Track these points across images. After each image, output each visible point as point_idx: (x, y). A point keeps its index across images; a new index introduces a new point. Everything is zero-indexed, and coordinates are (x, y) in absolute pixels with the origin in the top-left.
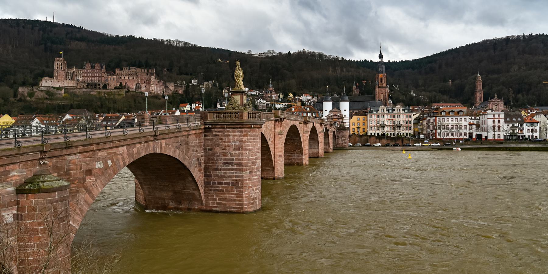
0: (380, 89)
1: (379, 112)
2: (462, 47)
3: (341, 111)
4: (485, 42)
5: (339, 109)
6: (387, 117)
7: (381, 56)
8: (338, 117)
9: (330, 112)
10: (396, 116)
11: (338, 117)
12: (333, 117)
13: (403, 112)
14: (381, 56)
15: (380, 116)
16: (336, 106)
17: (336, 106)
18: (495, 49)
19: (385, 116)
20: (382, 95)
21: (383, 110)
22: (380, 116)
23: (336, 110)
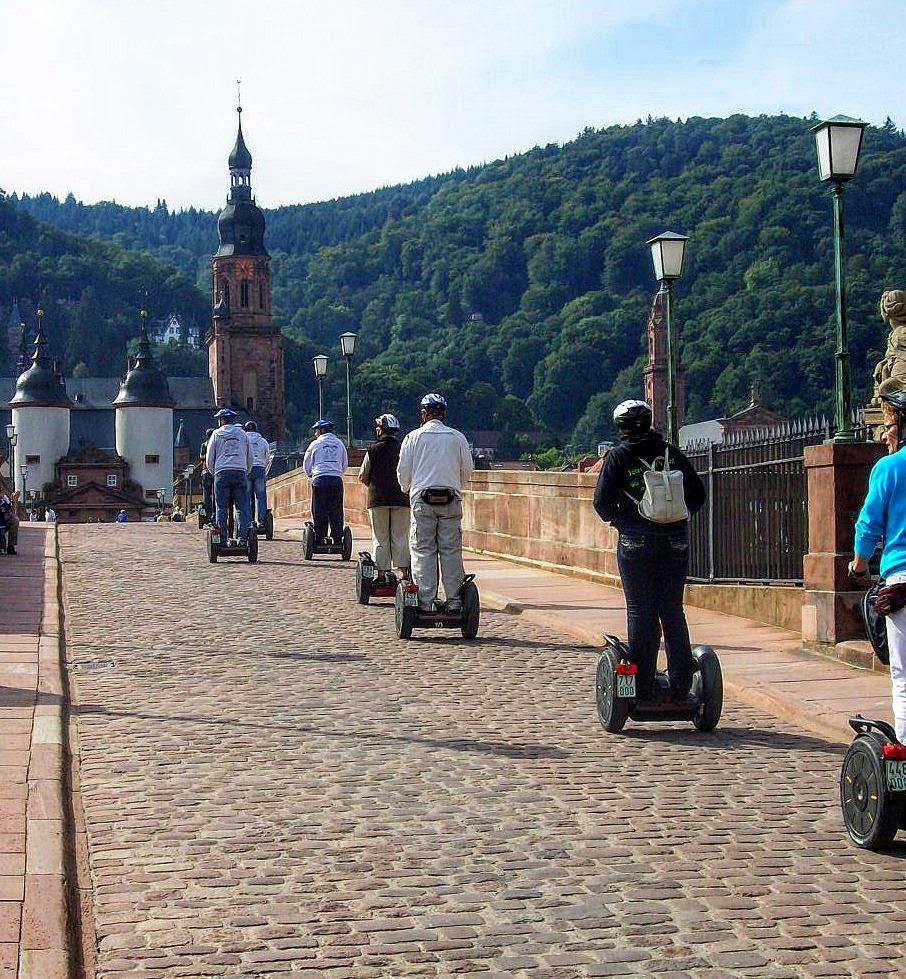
0: (238, 342)
7: (241, 161)
14: (241, 161)
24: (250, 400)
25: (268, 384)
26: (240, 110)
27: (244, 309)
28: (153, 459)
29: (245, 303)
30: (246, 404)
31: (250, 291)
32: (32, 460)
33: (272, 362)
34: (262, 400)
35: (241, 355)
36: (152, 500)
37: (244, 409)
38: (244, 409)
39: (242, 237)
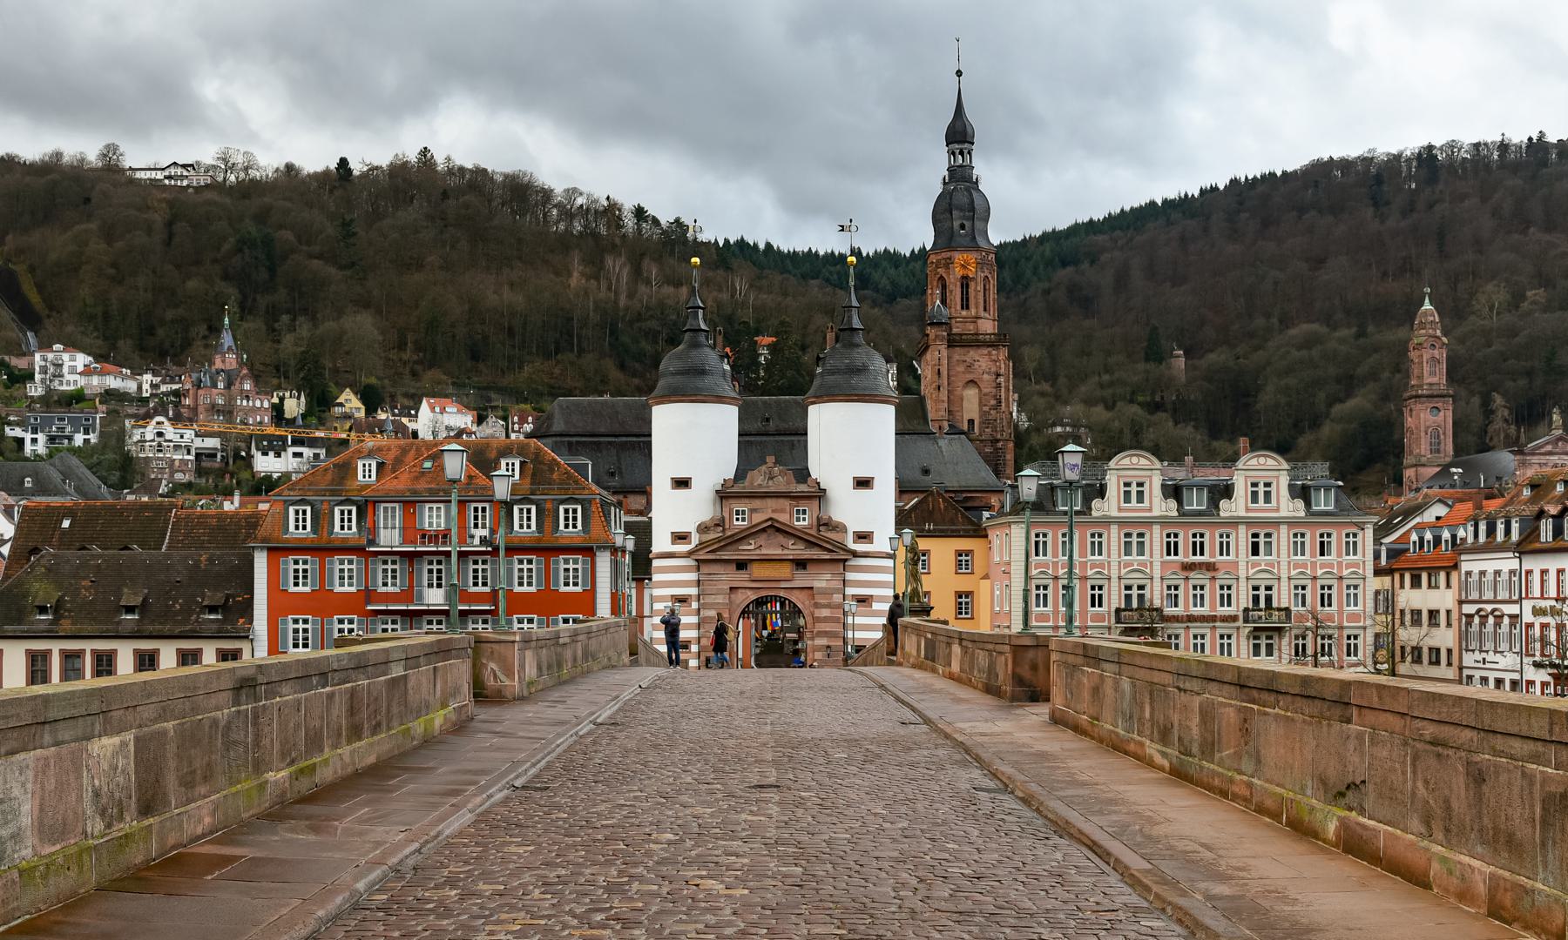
0: (958, 354)
1: (1107, 507)
2: (1214, 189)
3: (819, 495)
4: (1320, 172)
5: (803, 474)
6: (1172, 549)
7: (959, 135)
8: (797, 550)
9: (724, 495)
10: (1242, 538)
11: (797, 550)
12: (749, 549)
13: (1296, 509)
15: (1114, 536)
16: (773, 440)
17: (773, 440)
18: (1377, 202)
19: (1156, 537)
20: (971, 394)
21: (1134, 492)
22: (1114, 536)
23: (782, 482)
24: (971, 422)
25: (993, 402)
26: (959, 73)
27: (964, 313)
28: (863, 483)
29: (965, 305)
30: (965, 428)
31: (971, 290)
32: (682, 483)
33: (998, 375)
34: (986, 422)
35: (961, 368)
36: (860, 547)
37: (963, 433)
38: (963, 433)
39: (962, 227)
